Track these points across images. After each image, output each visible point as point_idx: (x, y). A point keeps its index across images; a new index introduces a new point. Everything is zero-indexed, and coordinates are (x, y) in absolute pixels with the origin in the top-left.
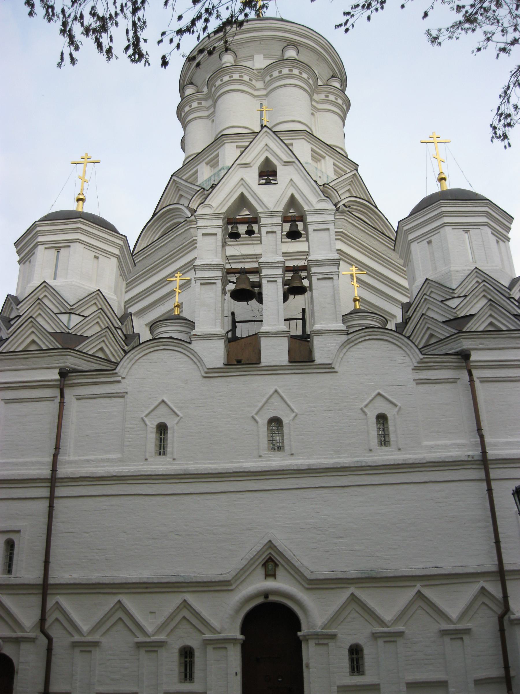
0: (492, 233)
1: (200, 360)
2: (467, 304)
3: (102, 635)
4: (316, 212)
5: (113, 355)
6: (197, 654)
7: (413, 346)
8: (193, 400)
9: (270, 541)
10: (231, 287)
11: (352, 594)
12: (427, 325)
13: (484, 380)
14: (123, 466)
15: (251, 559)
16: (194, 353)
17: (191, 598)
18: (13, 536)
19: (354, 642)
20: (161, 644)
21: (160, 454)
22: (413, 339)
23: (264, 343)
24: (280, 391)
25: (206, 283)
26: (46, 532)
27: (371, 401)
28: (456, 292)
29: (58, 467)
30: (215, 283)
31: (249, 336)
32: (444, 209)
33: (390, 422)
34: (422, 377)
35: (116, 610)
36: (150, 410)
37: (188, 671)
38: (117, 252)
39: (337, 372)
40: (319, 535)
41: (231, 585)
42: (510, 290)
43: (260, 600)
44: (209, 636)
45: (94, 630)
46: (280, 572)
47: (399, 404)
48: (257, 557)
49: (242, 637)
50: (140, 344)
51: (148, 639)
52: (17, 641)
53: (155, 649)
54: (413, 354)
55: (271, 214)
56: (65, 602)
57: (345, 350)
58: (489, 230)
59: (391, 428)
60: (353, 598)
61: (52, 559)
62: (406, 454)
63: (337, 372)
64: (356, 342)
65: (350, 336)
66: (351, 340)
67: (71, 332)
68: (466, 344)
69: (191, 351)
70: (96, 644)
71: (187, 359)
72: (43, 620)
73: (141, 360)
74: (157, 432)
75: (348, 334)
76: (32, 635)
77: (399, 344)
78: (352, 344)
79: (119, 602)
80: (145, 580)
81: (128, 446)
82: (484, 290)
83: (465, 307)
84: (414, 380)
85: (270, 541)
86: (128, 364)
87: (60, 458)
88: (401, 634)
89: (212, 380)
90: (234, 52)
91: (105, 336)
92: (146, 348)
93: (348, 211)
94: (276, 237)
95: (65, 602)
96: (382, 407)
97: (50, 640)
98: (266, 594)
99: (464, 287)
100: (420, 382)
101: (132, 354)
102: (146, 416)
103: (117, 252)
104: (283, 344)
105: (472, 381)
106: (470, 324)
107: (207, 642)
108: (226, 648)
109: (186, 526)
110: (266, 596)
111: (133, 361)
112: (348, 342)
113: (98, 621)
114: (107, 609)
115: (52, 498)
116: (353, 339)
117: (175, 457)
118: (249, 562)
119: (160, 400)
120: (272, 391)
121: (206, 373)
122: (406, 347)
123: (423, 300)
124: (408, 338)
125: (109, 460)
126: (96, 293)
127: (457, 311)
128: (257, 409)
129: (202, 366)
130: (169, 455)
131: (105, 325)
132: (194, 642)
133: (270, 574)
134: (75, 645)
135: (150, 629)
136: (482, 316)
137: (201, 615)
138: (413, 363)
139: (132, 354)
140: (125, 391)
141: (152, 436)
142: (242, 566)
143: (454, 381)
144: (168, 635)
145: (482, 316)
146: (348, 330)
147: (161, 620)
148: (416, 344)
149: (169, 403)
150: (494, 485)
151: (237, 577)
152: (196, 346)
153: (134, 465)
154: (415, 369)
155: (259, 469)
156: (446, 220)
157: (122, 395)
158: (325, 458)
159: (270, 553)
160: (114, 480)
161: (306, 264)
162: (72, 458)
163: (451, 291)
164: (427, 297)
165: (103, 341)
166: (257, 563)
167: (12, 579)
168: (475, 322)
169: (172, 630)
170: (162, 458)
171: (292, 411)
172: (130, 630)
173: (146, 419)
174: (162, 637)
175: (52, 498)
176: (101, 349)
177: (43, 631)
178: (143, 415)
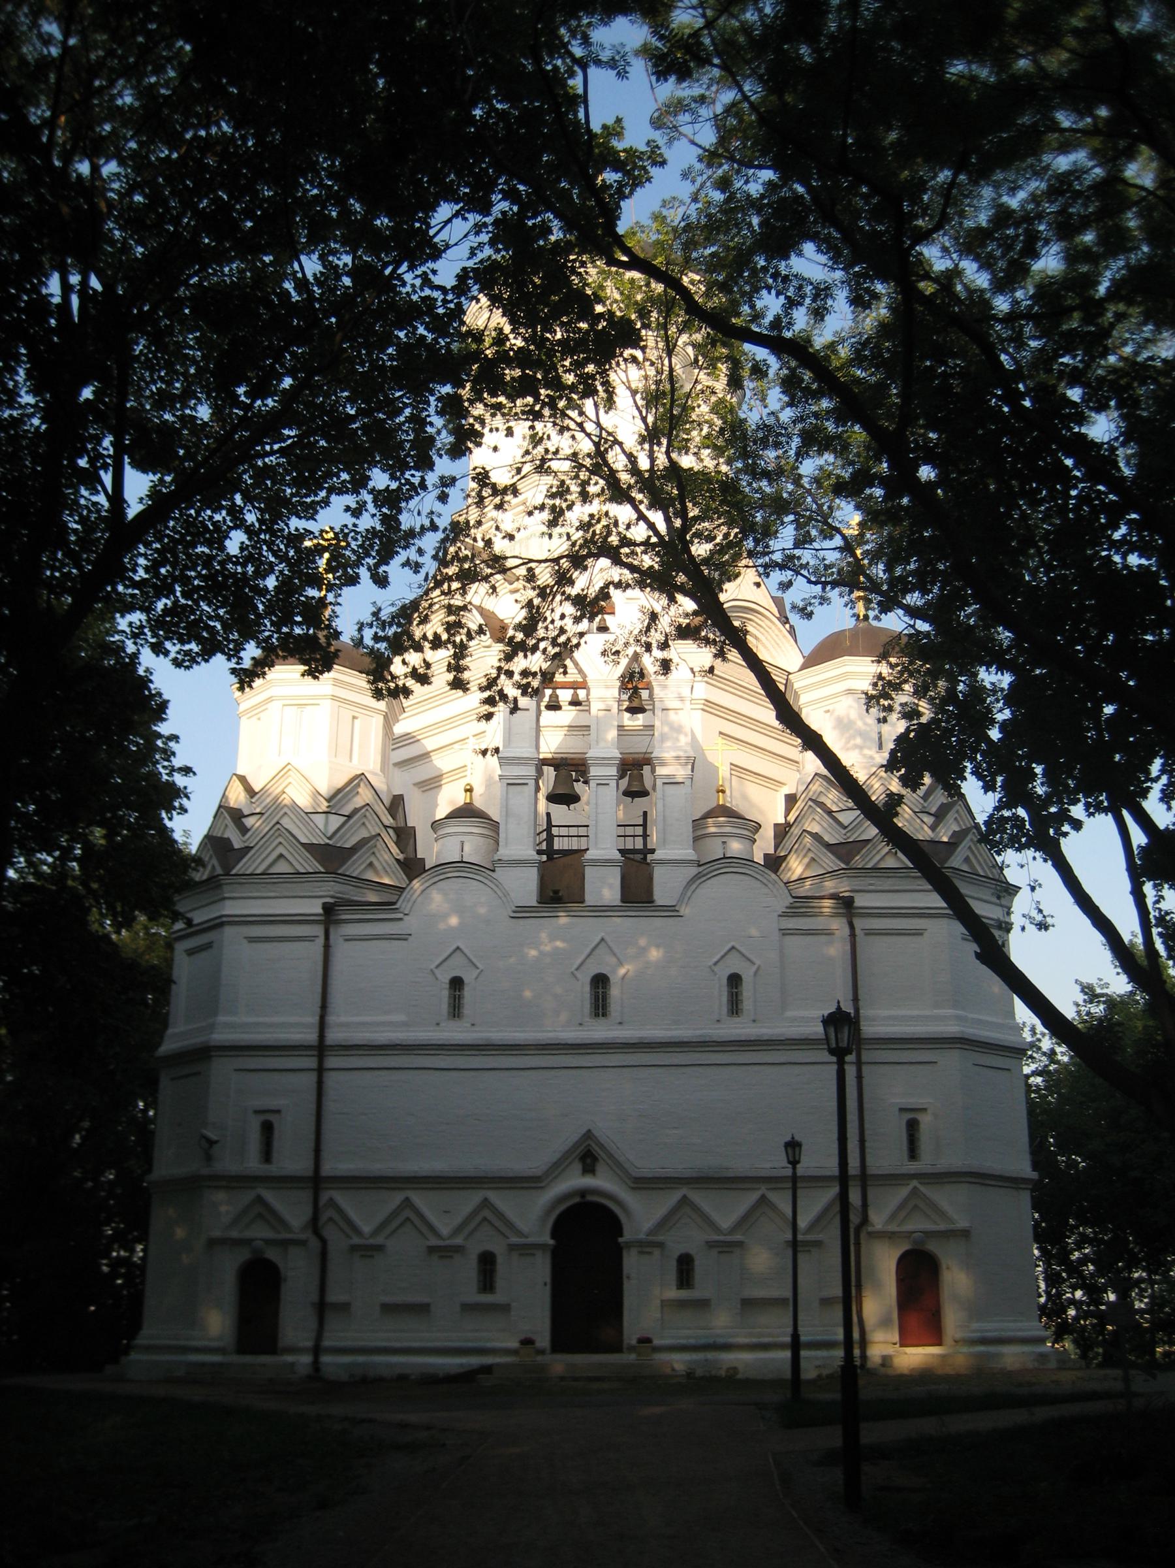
11: (685, 1197)
16: (498, 885)
17: (493, 1196)
19: (683, 1251)
20: (459, 1249)
26: (314, 1112)
27: (723, 957)
34: (790, 926)
43: (577, 1200)
44: (515, 1240)
46: (600, 1168)
47: (758, 962)
49: (552, 1242)
50: (425, 871)
52: (285, 1244)
65: (701, 869)
67: (330, 842)
70: (380, 1248)
75: (700, 866)
76: (303, 1236)
79: (407, 1199)
80: (438, 1174)
89: (521, 921)
95: (340, 1198)
96: (734, 965)
97: (324, 1242)
98: (583, 1193)
102: (437, 967)
104: (614, 877)
107: (512, 1248)
115: (321, 1070)
119: (454, 947)
120: (598, 939)
125: (391, 1024)
132: (497, 1246)
134: (354, 1248)
135: (445, 1231)
144: (466, 1239)
147: (458, 1220)
149: (466, 951)
150: (865, 1069)
152: (500, 873)
154: (784, 915)
157: (403, 938)
162: (343, 1019)
167: (273, 1169)
172: (420, 1232)
173: (436, 971)
174: (458, 1241)
175: (321, 1070)
177: (317, 1232)
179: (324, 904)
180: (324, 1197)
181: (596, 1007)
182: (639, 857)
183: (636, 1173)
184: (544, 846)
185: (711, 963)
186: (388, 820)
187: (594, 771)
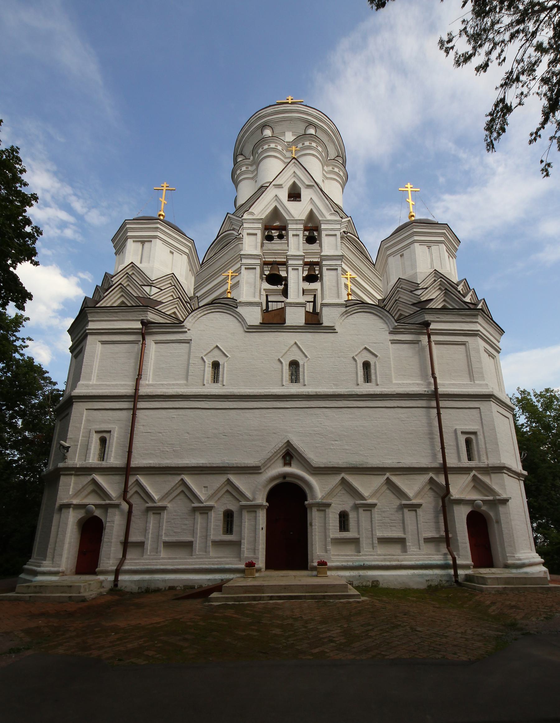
0: (447, 251)
1: (244, 320)
2: (428, 293)
3: (169, 502)
5: (182, 316)
6: (235, 515)
7: (391, 317)
8: (238, 346)
9: (288, 441)
10: (267, 273)
11: (343, 478)
12: (399, 308)
13: (438, 343)
14: (188, 388)
15: (275, 452)
16: (240, 315)
20: (210, 508)
21: (214, 383)
22: (391, 312)
23: (288, 310)
24: (298, 343)
25: (250, 268)
27: (360, 352)
28: (420, 285)
29: (140, 388)
30: (255, 268)
31: (277, 309)
32: (415, 230)
33: (372, 367)
34: (395, 338)
35: (180, 486)
36: (207, 352)
37: (229, 526)
38: (187, 251)
39: (337, 332)
40: (322, 438)
41: (260, 469)
42: (458, 286)
44: (244, 503)
45: (162, 499)
48: (279, 451)
51: (201, 505)
53: (207, 512)
54: (390, 323)
55: (297, 222)
57: (343, 318)
58: (445, 247)
61: (134, 451)
62: (382, 388)
63: (337, 332)
64: (351, 313)
66: (348, 311)
68: (428, 318)
70: (164, 508)
71: (234, 319)
72: (125, 491)
73: (201, 318)
74: (212, 368)
75: (346, 307)
77: (381, 316)
78: (349, 314)
79: (182, 480)
80: (201, 465)
81: (191, 375)
82: (440, 284)
83: (426, 295)
84: (390, 340)
85: (288, 441)
86: (192, 320)
87: (142, 382)
90: (271, 127)
91: (177, 304)
92: (205, 309)
93: (346, 237)
94: (299, 239)
98: (285, 476)
99: (426, 282)
100: (393, 342)
101: (195, 313)
102: (205, 355)
103: (187, 251)
105: (429, 342)
106: (430, 304)
107: (243, 508)
108: (256, 512)
109: (231, 429)
111: (196, 319)
112: (346, 312)
113: (166, 492)
114: (173, 484)
116: (350, 310)
117: (224, 384)
118: (273, 454)
119: (215, 345)
120: (293, 343)
121: (248, 329)
122: (386, 318)
123: (396, 291)
124: (388, 312)
125: (178, 384)
126: (171, 275)
127: (421, 297)
128: (282, 355)
129: (244, 324)
130: (220, 382)
131: (176, 296)
133: (287, 463)
134: (148, 509)
136: (439, 300)
137: (239, 489)
138: (389, 329)
139: (195, 313)
140: (190, 338)
141: (209, 370)
142: (269, 457)
143: (417, 342)
145: (439, 300)
146: (346, 304)
147: (210, 492)
148: (393, 315)
150: (442, 411)
151: (265, 464)
152: (240, 310)
153: (196, 388)
155: (282, 394)
156: (416, 238)
157: (188, 342)
158: (327, 388)
159: (288, 449)
160: (181, 398)
161: (319, 261)
163: (417, 285)
164: (399, 289)
165: (176, 307)
166: (279, 456)
168: (434, 304)
169: (219, 499)
170: (215, 384)
171: (306, 357)
172: (189, 498)
173: (204, 358)
176: (174, 313)
178: (203, 355)
185: (354, 355)
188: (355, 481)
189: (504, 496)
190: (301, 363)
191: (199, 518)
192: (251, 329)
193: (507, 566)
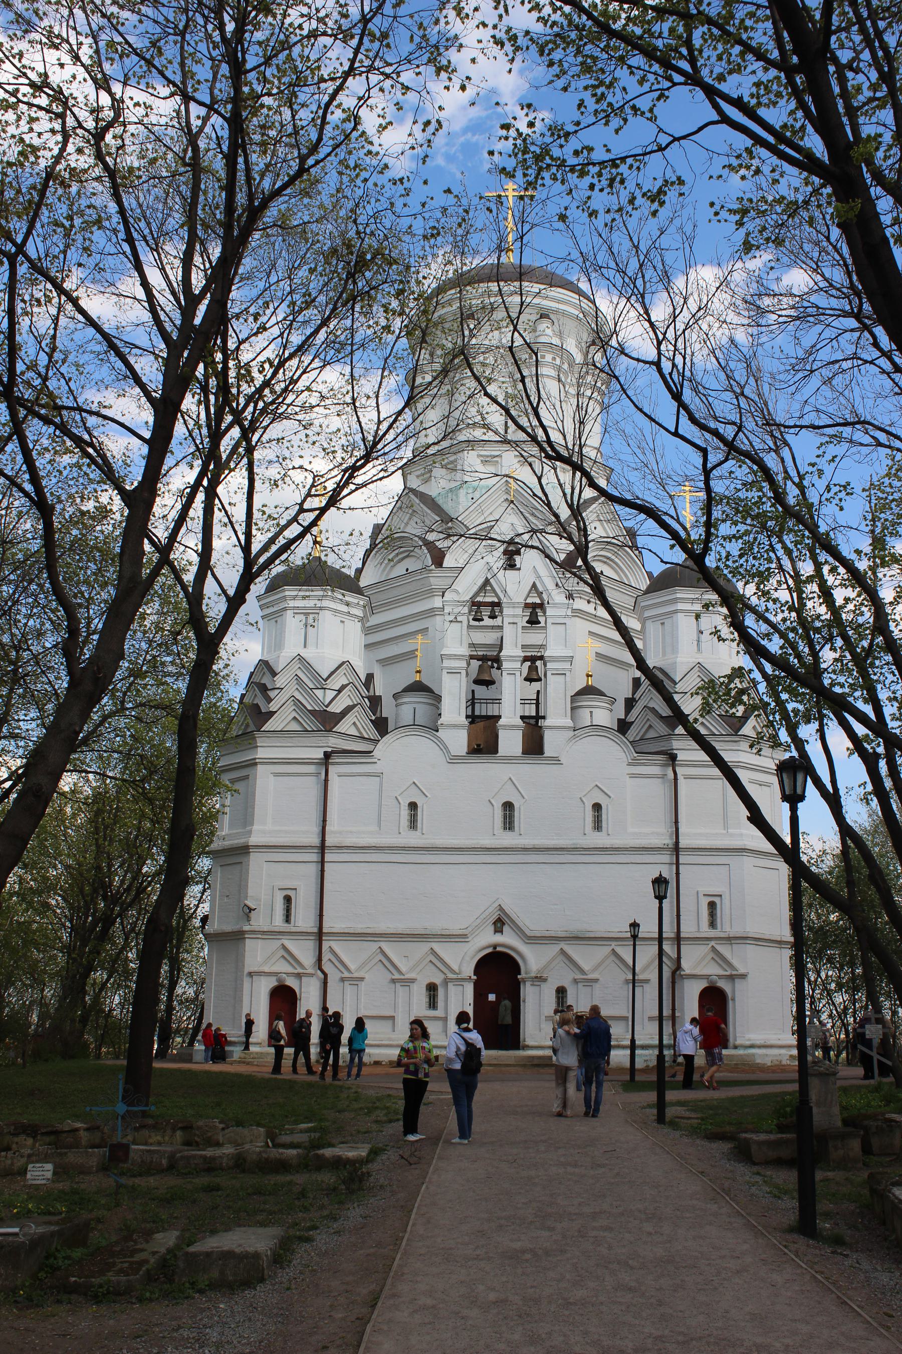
1: (446, 748)
4: (556, 605)
13: (687, 777)
16: (441, 741)
18: (291, 893)
20: (413, 981)
43: (490, 950)
52: (299, 976)
56: (337, 946)
59: (604, 817)
60: (562, 952)
69: (437, 738)
88: (596, 980)
95: (337, 946)
97: (325, 975)
110: (495, 947)
132: (437, 980)
135: (403, 969)
141: (405, 813)
170: (412, 833)
179: (325, 753)
180: (325, 946)
181: (505, 823)
182: (532, 721)
183: (529, 933)
184: (470, 713)
186: (365, 692)
187: (505, 665)
188: (573, 951)
189: (742, 971)
190: (516, 806)
191: (401, 990)
192: (454, 760)
193: (736, 1047)
